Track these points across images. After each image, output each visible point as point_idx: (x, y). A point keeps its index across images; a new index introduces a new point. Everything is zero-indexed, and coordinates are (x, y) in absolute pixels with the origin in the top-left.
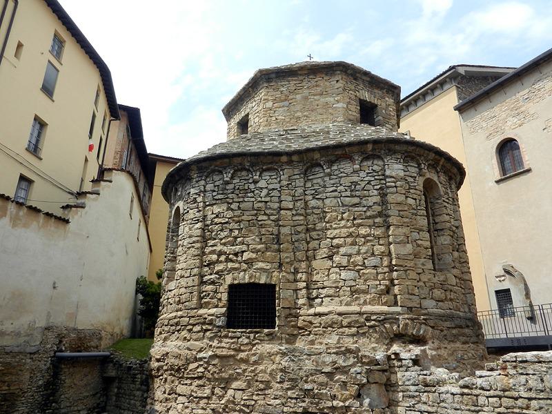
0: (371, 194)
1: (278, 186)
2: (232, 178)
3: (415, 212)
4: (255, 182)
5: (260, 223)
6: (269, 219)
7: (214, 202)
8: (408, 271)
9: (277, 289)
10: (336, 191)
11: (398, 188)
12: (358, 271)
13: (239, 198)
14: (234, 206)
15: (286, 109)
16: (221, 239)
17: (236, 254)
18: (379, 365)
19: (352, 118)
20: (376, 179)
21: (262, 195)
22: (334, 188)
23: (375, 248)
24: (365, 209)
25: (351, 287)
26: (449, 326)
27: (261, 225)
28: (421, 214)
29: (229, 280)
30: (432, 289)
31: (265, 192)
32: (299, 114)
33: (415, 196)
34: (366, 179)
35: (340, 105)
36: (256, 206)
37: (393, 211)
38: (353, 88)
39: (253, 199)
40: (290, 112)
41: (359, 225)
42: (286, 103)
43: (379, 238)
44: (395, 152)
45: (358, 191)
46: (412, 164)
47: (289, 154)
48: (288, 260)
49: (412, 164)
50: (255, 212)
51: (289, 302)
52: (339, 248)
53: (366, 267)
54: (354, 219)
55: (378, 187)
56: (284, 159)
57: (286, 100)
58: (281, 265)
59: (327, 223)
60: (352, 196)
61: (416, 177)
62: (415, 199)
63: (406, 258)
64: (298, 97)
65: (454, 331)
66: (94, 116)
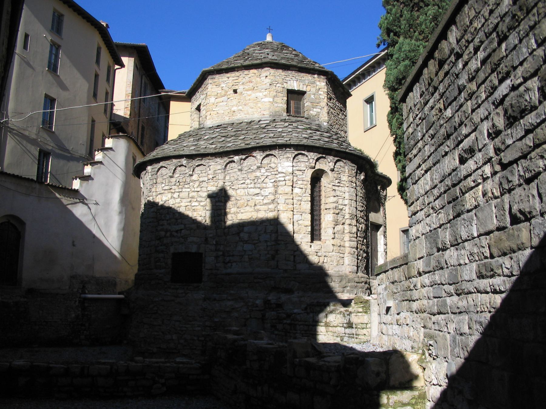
0: (268, 186)
1: (206, 179)
3: (300, 198)
5: (193, 208)
6: (199, 204)
7: (163, 192)
9: (204, 256)
10: (244, 183)
11: (287, 182)
12: (254, 244)
13: (179, 188)
14: (176, 195)
15: (225, 103)
16: (168, 220)
17: (177, 231)
18: (257, 307)
21: (195, 186)
22: (243, 181)
24: (263, 198)
25: (249, 255)
28: (305, 200)
29: (172, 250)
31: (197, 184)
32: (235, 108)
33: (301, 186)
35: (267, 100)
36: (190, 195)
38: (281, 81)
39: (189, 190)
41: (258, 210)
42: (225, 98)
45: (259, 183)
48: (211, 235)
49: (302, 160)
52: (244, 227)
53: (260, 241)
55: (273, 181)
58: (206, 239)
59: (238, 208)
60: (255, 188)
66: (97, 76)
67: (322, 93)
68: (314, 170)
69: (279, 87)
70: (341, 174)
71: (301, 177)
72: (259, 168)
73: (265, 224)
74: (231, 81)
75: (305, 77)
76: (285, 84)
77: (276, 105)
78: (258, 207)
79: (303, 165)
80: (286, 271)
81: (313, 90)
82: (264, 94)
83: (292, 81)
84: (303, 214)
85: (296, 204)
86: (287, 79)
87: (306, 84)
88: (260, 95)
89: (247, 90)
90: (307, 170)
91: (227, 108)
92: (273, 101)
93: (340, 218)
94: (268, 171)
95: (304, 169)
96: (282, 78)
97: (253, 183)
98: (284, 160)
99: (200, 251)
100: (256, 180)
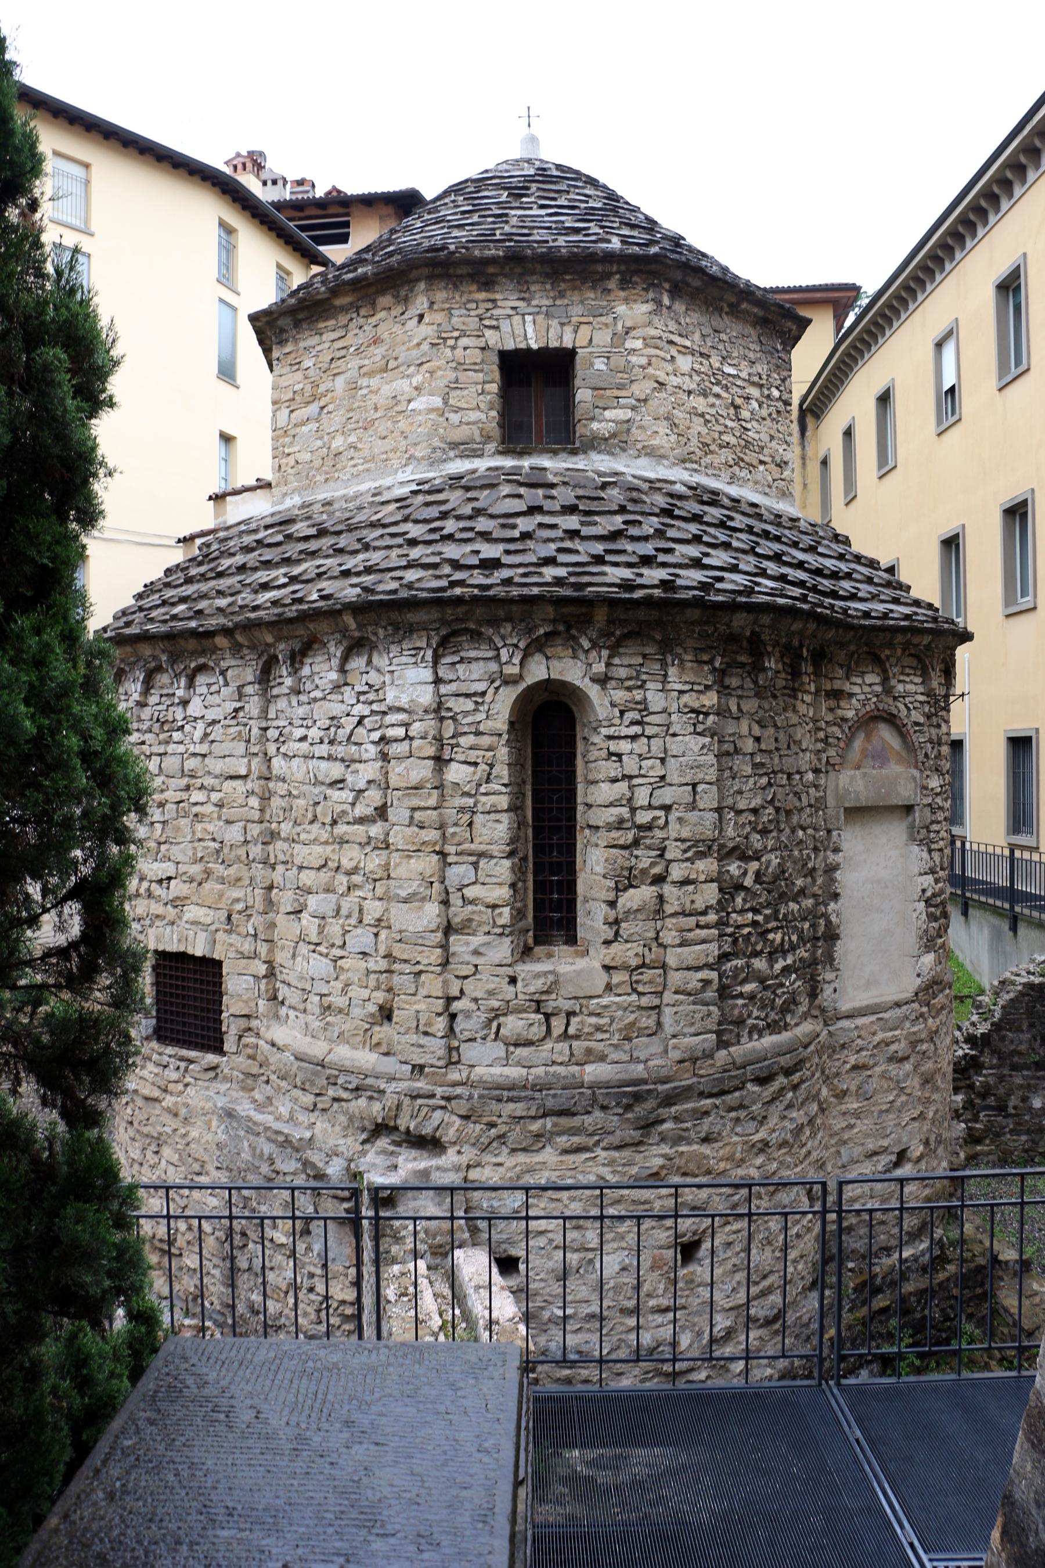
0: (365, 756)
2: (146, 691)
3: (470, 802)
4: (185, 703)
5: (196, 809)
8: (423, 977)
10: (303, 739)
11: (416, 743)
19: (457, 435)
20: (373, 712)
23: (366, 904)
25: (322, 995)
26: (518, 1114)
27: (196, 815)
30: (497, 1014)
32: (338, 443)
33: (472, 756)
34: (361, 709)
37: (398, 813)
38: (473, 323)
39: (181, 749)
40: (321, 438)
41: (343, 842)
43: (375, 880)
44: (411, 630)
46: (472, 654)
47: (227, 632)
49: (472, 654)
50: (185, 781)
51: (246, 1002)
54: (334, 822)
55: (376, 736)
56: (221, 641)
57: (314, 398)
60: (330, 758)
61: (483, 694)
62: (476, 764)
63: (420, 941)
64: (340, 382)
65: (535, 1126)
67: (638, 344)
68: (522, 686)
69: (468, 350)
70: (649, 685)
71: (469, 719)
72: (337, 688)
73: (361, 894)
74: (327, 345)
75: (569, 293)
76: (488, 333)
77: (455, 418)
78: (341, 829)
79: (478, 670)
80: (419, 1069)
81: (603, 338)
82: (416, 380)
83: (517, 319)
84: (482, 863)
85: (456, 825)
86: (496, 312)
87: (574, 319)
88: (403, 386)
89: (370, 374)
90: (491, 691)
91: (319, 443)
92: (446, 402)
93: (644, 858)
94: (362, 698)
95: (481, 687)
96: (480, 311)
97: (326, 741)
98: (404, 659)
99: (216, 957)
100: (333, 729)
